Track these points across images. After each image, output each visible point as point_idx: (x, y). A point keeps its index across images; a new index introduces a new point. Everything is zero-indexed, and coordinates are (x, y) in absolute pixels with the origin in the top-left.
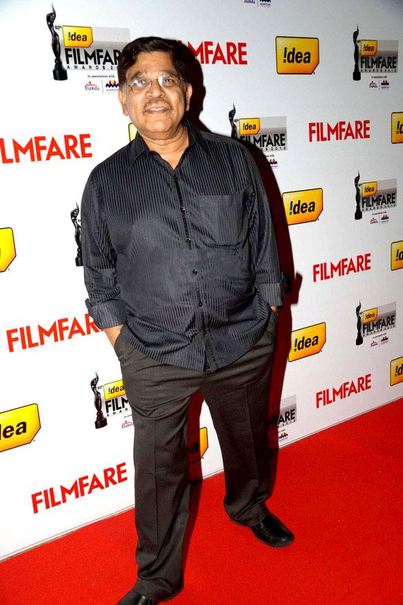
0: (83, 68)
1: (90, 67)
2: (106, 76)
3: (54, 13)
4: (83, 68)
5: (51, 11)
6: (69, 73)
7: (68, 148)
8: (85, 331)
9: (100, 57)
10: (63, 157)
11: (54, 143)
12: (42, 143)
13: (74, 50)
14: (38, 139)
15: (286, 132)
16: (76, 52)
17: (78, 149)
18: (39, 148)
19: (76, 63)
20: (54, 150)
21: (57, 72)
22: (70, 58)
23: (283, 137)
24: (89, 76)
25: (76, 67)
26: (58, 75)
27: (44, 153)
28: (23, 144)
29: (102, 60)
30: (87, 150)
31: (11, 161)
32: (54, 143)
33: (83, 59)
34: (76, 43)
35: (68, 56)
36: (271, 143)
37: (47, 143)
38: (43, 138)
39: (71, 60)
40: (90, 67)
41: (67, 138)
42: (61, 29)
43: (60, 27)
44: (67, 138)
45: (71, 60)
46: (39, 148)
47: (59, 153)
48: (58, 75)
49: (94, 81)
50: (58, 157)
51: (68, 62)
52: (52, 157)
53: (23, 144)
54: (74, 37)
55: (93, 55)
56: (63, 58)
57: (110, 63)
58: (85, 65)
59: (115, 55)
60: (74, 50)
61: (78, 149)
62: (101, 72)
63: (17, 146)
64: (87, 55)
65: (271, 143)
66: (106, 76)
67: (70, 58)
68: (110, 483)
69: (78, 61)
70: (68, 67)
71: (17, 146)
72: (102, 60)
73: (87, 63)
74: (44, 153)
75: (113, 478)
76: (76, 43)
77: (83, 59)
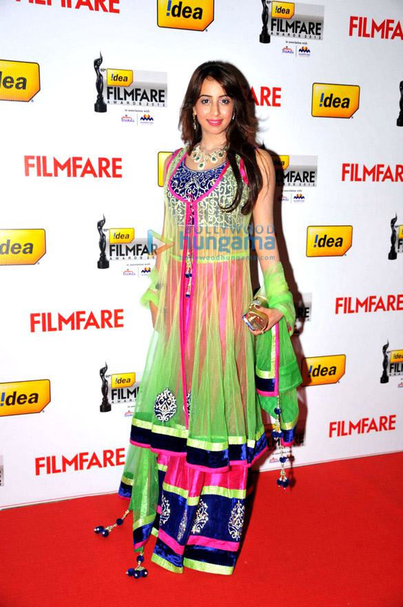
0: (122, 103)
1: (128, 103)
2: (142, 111)
3: (101, 59)
4: (122, 103)
5: (99, 57)
6: (109, 107)
8: (100, 325)
9: (137, 95)
10: (95, 176)
12: (78, 163)
13: (115, 88)
15: (316, 170)
16: (117, 90)
19: (115, 99)
21: (98, 105)
22: (110, 95)
23: (313, 175)
24: (126, 110)
25: (115, 102)
26: (98, 108)
29: (139, 97)
31: (50, 175)
33: (122, 96)
34: (117, 83)
35: (109, 93)
36: (300, 179)
39: (112, 96)
40: (128, 103)
42: (105, 71)
43: (105, 70)
44: (101, 160)
45: (112, 96)
48: (98, 108)
49: (129, 114)
50: (91, 175)
51: (108, 98)
52: (86, 175)
54: (116, 78)
55: (132, 92)
56: (105, 94)
57: (146, 100)
58: (123, 101)
59: (152, 93)
60: (115, 88)
62: (137, 107)
64: (126, 92)
65: (300, 179)
66: (142, 111)
67: (110, 95)
68: (108, 463)
69: (117, 97)
70: (108, 102)
71: (56, 163)
72: (139, 97)
73: (125, 99)
75: (112, 460)
76: (117, 83)
77: (122, 96)
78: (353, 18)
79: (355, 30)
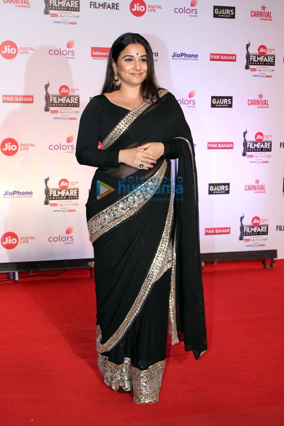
7: (112, 6)
11: (109, 5)
14: (105, 3)
17: (115, 7)
18: (105, 6)
20: (109, 7)
27: (106, 7)
28: (101, 4)
30: (118, 8)
32: (109, 5)
37: (107, 5)
38: (106, 3)
41: (112, 4)
46: (105, 6)
47: (110, 7)
53: (101, 4)
61: (115, 7)
63: (99, 4)
74: (106, 7)
78: (91, 2)
79: (92, 6)
